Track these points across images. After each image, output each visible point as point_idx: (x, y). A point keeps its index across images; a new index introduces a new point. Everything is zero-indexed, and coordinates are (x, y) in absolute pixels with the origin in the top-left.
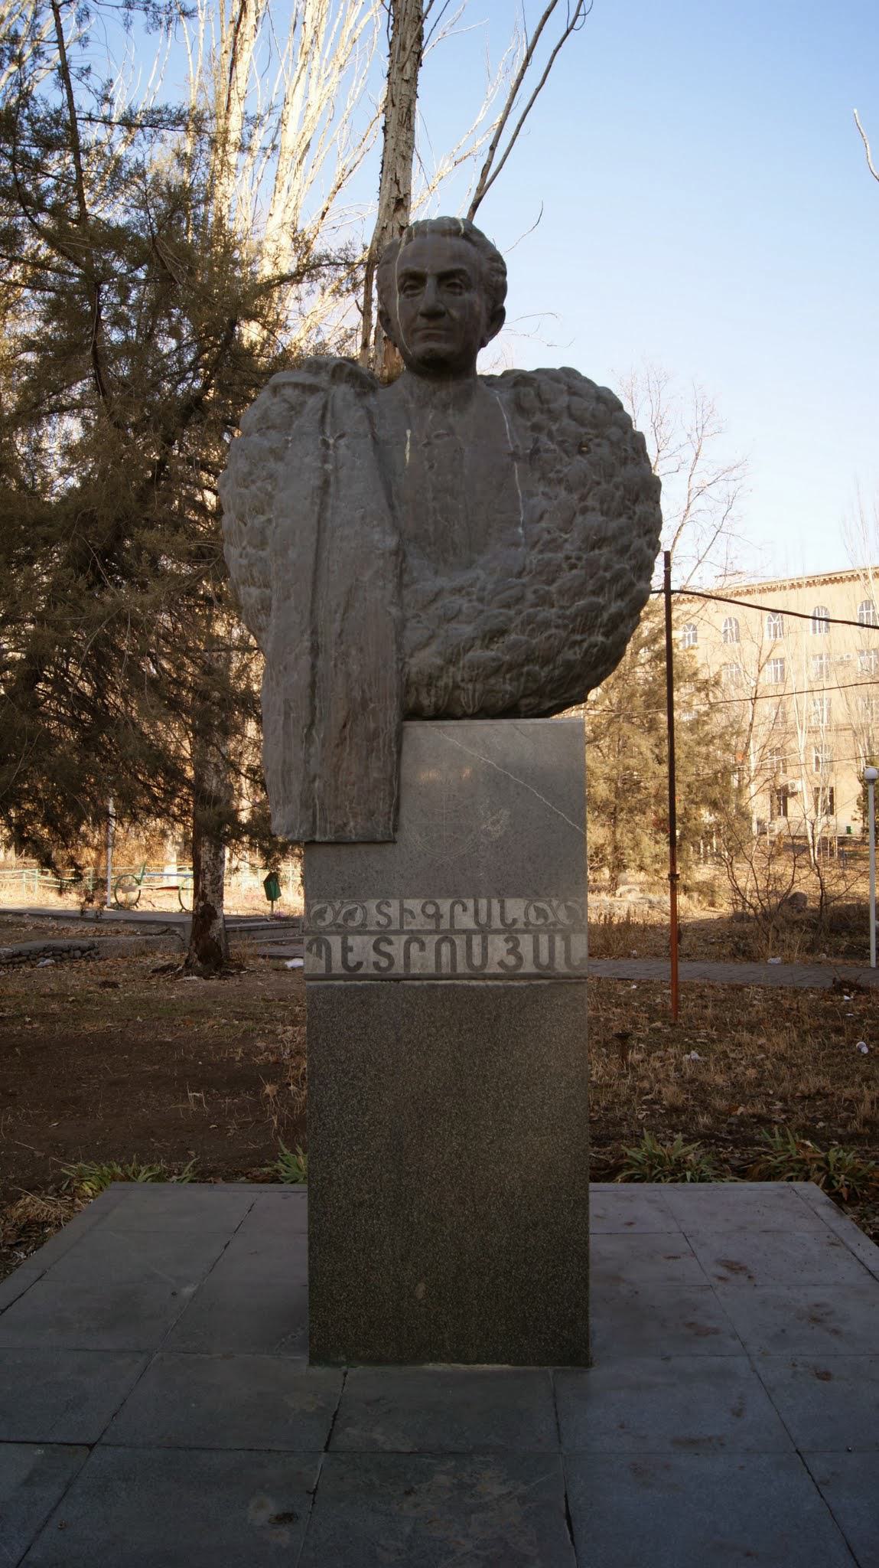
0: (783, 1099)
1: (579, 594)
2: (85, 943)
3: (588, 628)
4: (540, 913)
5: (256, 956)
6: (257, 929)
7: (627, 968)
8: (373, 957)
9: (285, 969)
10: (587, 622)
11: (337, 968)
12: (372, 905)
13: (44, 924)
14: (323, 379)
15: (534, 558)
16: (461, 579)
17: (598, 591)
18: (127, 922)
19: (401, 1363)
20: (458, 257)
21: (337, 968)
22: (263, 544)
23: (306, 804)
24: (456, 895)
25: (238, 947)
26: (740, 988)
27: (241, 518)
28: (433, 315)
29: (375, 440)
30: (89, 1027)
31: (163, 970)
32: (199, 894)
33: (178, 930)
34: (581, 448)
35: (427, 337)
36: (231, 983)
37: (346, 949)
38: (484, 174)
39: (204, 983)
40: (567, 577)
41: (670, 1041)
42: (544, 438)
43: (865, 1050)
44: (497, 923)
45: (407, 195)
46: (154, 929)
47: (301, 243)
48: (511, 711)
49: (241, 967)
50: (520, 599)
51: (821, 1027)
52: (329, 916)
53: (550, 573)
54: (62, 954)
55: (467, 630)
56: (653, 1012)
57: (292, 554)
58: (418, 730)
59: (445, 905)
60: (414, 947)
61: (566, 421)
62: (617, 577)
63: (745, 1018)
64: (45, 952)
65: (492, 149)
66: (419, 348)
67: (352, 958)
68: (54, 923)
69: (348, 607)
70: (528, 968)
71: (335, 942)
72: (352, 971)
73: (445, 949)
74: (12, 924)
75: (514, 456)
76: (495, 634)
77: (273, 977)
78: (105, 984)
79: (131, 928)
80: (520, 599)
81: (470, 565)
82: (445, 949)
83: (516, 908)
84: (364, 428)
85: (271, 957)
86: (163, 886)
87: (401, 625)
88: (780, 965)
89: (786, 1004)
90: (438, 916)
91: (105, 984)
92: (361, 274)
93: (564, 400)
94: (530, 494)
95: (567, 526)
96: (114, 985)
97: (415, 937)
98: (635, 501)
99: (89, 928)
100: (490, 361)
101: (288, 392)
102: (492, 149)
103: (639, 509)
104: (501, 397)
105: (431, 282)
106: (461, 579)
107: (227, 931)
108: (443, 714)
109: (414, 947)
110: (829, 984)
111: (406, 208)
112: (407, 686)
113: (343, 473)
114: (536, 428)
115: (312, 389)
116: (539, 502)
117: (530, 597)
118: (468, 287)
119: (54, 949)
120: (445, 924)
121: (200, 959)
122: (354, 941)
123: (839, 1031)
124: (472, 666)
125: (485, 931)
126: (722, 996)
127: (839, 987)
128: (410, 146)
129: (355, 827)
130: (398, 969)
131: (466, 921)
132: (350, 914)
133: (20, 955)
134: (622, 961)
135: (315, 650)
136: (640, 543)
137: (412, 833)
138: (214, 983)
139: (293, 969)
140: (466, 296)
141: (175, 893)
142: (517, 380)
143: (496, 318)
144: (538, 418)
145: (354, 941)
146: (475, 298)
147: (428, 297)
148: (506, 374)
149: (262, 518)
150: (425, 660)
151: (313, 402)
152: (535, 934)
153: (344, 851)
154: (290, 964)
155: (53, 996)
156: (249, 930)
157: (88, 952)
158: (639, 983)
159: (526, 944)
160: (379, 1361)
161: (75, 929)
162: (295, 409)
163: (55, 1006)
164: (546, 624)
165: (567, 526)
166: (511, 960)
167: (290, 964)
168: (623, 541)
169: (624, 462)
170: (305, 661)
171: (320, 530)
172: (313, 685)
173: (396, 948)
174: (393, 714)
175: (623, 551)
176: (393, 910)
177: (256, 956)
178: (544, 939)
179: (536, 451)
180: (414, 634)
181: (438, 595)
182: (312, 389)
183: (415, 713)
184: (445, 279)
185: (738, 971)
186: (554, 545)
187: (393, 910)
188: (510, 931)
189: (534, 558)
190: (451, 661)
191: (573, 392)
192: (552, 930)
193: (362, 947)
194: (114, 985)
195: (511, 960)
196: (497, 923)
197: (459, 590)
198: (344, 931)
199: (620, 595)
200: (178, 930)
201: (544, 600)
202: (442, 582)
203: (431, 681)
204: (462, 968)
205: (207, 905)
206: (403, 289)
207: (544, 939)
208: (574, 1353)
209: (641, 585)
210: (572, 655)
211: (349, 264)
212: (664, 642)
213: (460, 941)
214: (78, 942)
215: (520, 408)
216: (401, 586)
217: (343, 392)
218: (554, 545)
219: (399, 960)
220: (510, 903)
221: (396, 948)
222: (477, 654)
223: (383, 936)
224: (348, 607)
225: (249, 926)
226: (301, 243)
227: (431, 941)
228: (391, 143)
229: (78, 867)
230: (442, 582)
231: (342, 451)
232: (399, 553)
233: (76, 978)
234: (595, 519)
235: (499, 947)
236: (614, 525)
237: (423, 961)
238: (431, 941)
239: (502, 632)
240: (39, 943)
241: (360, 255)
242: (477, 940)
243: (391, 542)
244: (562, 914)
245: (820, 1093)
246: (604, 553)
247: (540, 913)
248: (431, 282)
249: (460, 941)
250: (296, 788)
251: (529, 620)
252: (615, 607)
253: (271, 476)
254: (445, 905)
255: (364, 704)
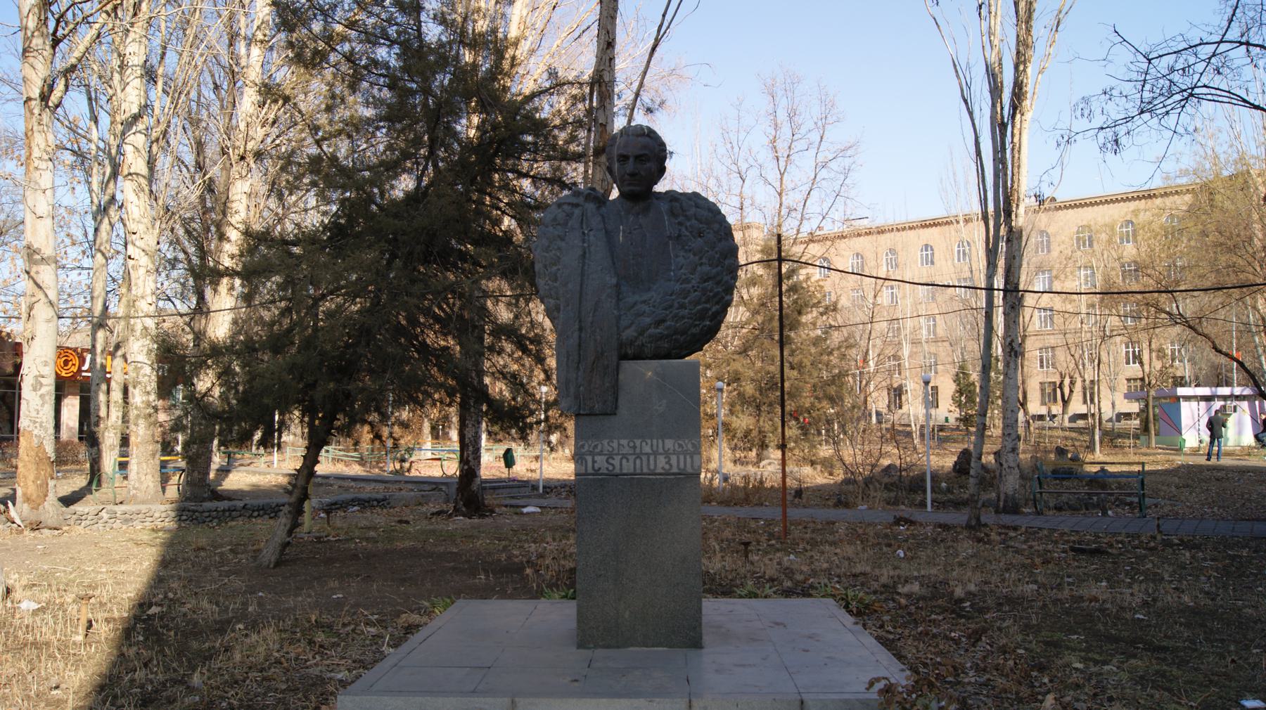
0: (839, 576)
1: (698, 303)
2: (380, 496)
3: (702, 318)
4: (680, 446)
5: (500, 506)
6: (499, 488)
7: (758, 512)
8: (606, 465)
9: (522, 513)
10: (702, 315)
11: (590, 470)
12: (605, 442)
13: (346, 484)
14: (581, 200)
15: (678, 287)
16: (645, 297)
17: (707, 302)
18: (406, 482)
19: (618, 647)
20: (645, 147)
21: (590, 470)
22: (556, 280)
23: (577, 397)
24: (643, 438)
25: (489, 499)
26: (834, 523)
27: (545, 266)
28: (632, 175)
29: (606, 232)
30: (399, 545)
31: (439, 513)
32: (463, 461)
33: (444, 488)
34: (700, 234)
35: (629, 185)
36: (488, 520)
37: (594, 462)
38: (659, 31)
39: (468, 521)
40: (694, 295)
41: (778, 550)
42: (683, 229)
43: (902, 555)
44: (661, 450)
45: (614, 39)
46: (427, 487)
47: (552, 73)
48: (668, 356)
49: (492, 511)
50: (671, 306)
51: (879, 544)
52: (586, 447)
53: (685, 293)
54: (365, 504)
55: (648, 320)
56: (771, 536)
57: (570, 286)
58: (627, 365)
59: (638, 442)
60: (624, 461)
61: (694, 221)
62: (714, 296)
63: (831, 538)
64: (354, 502)
65: (664, 16)
66: (627, 189)
67: (597, 466)
68: (352, 484)
69: (595, 310)
70: (675, 470)
71: (589, 459)
72: (597, 472)
73: (638, 462)
74: (321, 485)
75: (670, 238)
76: (659, 323)
77: (516, 517)
78: (400, 522)
79: (410, 486)
80: (671, 306)
81: (649, 289)
82: (638, 462)
83: (669, 444)
84: (601, 226)
85: (512, 506)
86: (433, 459)
87: (618, 318)
88: (874, 513)
89: (860, 531)
90: (635, 447)
91: (400, 522)
92: (587, 90)
93: (693, 210)
94: (677, 256)
95: (693, 271)
96: (407, 522)
97: (624, 456)
98: (725, 258)
99: (381, 487)
100: (660, 187)
101: (566, 207)
102: (664, 16)
103: (727, 262)
104: (664, 207)
105: (631, 159)
106: (645, 297)
107: (485, 488)
108: (637, 357)
109: (624, 461)
110: (892, 520)
111: (613, 47)
112: (621, 345)
113: (592, 248)
114: (680, 224)
115: (577, 205)
116: (681, 260)
117: (676, 305)
118: (649, 160)
119: (359, 500)
120: (638, 451)
121: (464, 505)
122: (597, 458)
123: (889, 545)
124: (650, 336)
125: (655, 453)
126: (819, 527)
127: (898, 521)
128: (615, 10)
129: (598, 407)
130: (617, 471)
131: (647, 449)
132: (596, 446)
133: (336, 504)
134: (756, 508)
135: (581, 329)
136: (726, 278)
137: (623, 410)
138: (476, 521)
139: (528, 514)
140: (648, 165)
141: (439, 463)
142: (672, 196)
143: (662, 170)
144: (681, 219)
145: (597, 458)
146: (652, 165)
147: (630, 166)
148: (667, 192)
149: (555, 268)
150: (629, 333)
151: (577, 211)
152: (678, 454)
153: (593, 418)
154: (525, 510)
155: (369, 528)
156: (494, 488)
157: (382, 503)
158: (766, 520)
159: (674, 459)
160: (608, 647)
161: (369, 487)
162: (569, 215)
163: (372, 534)
164: (683, 317)
165: (693, 271)
166: (667, 467)
167: (525, 510)
168: (719, 278)
169: (720, 240)
170: (576, 334)
171: (582, 274)
172: (580, 345)
173: (616, 462)
174: (615, 359)
175: (718, 283)
176: (615, 445)
177: (500, 506)
178: (682, 457)
179: (679, 236)
180: (624, 323)
181: (635, 304)
182: (577, 205)
183: (624, 357)
184: (638, 158)
185: (832, 513)
186: (687, 281)
187: (615, 445)
188: (667, 454)
189: (678, 287)
190: (641, 333)
191: (697, 206)
192: (685, 453)
193: (601, 461)
194: (407, 522)
195: (667, 467)
196: (661, 450)
197: (644, 302)
198: (592, 454)
199: (717, 303)
200: (444, 488)
201: (682, 306)
202: (637, 298)
203: (632, 343)
204: (645, 470)
205: (470, 468)
206: (619, 161)
207: (682, 457)
208: (696, 644)
209: (728, 298)
210: (694, 330)
211: (581, 84)
212: (784, 288)
213: (645, 458)
214: (375, 496)
215: (672, 213)
216: (619, 300)
217: (591, 207)
218: (687, 281)
219: (618, 467)
220: (667, 441)
221: (616, 462)
222: (652, 331)
223: (610, 456)
224: (595, 310)
225: (497, 485)
226: (552, 73)
227: (632, 458)
228: (605, 13)
229: (395, 439)
230: (637, 298)
231: (592, 238)
232: (618, 285)
233: (379, 518)
234: (706, 268)
235: (662, 461)
236: (714, 271)
237: (628, 467)
238: (632, 458)
239: (663, 321)
240: (349, 496)
241: (586, 77)
242: (652, 458)
243: (614, 281)
244: (690, 446)
245: (864, 574)
246: (709, 285)
247: (680, 446)
248: (631, 159)
249: (645, 458)
250: (572, 390)
251: (675, 316)
252: (714, 309)
253: (559, 249)
254: (638, 442)
255: (602, 354)
